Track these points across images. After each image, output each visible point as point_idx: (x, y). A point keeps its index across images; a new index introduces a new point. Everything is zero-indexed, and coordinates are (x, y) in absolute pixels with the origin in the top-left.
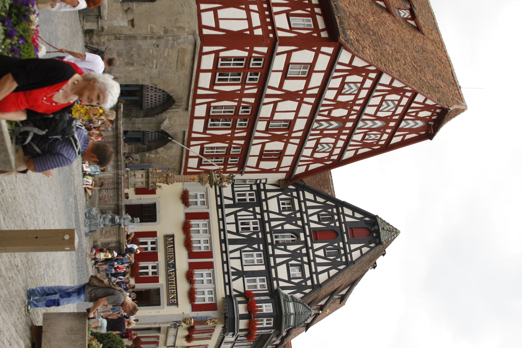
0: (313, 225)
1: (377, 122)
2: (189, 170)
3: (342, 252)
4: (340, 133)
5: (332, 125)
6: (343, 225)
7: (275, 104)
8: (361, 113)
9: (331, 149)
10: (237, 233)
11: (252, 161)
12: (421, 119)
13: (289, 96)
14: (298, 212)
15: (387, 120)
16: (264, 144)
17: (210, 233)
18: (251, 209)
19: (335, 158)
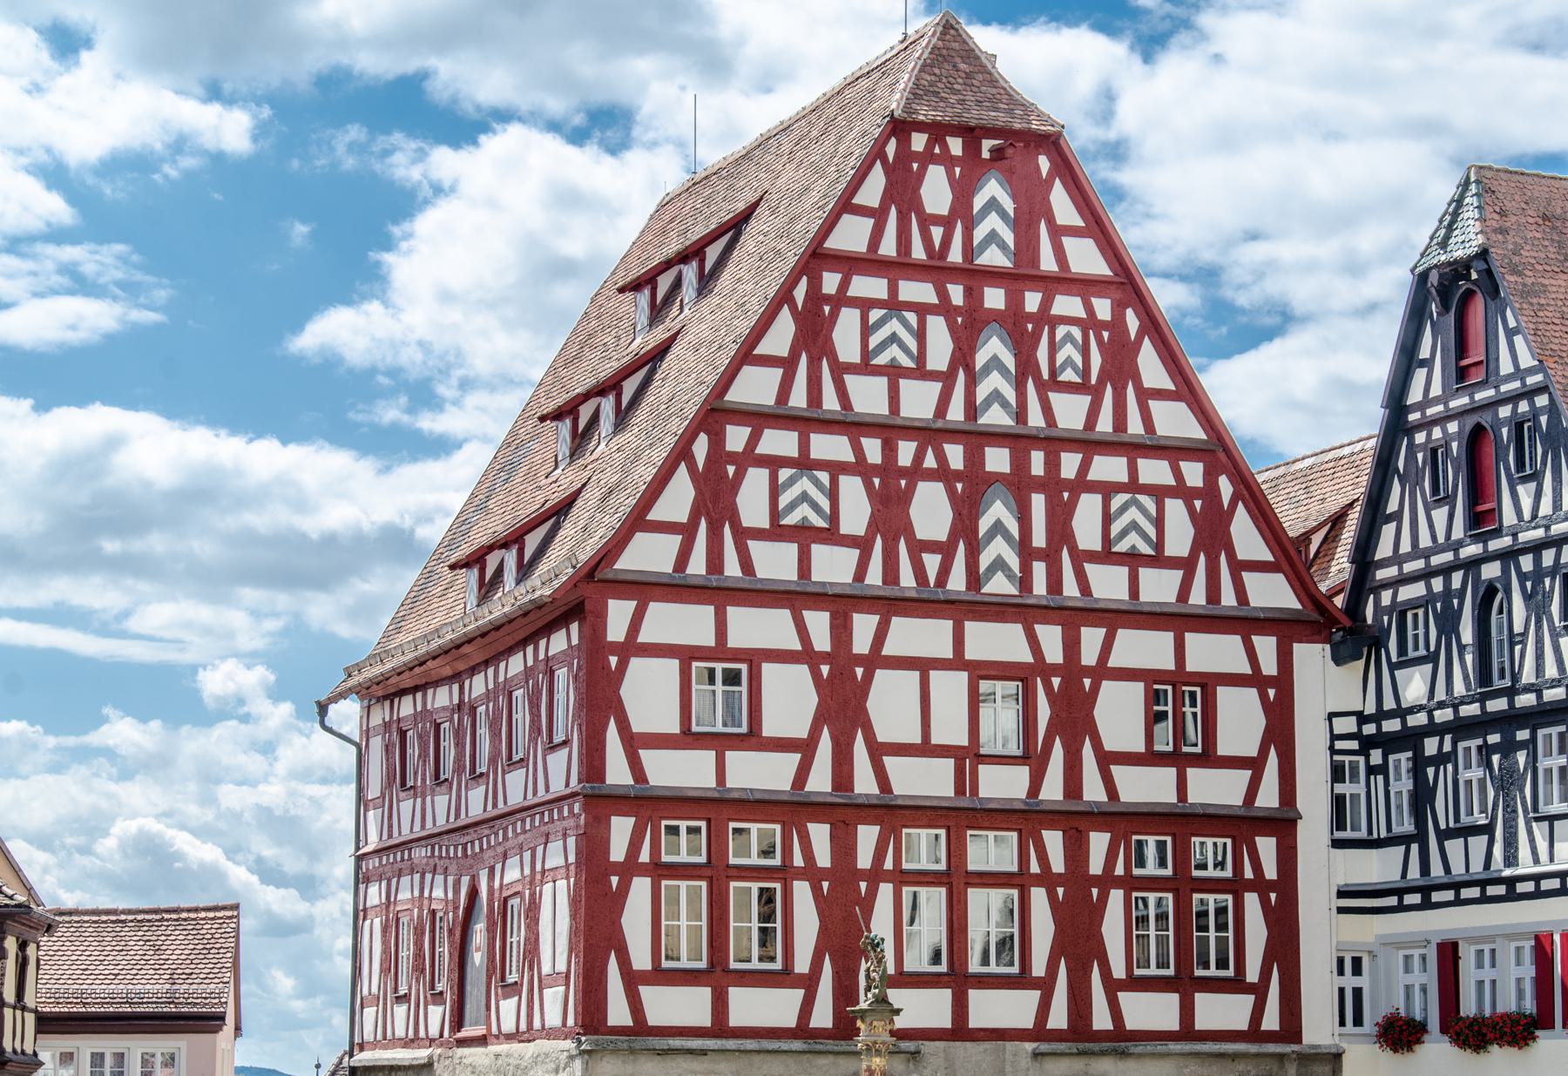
0: (1458, 532)
1: (981, 359)
2: (1271, 1021)
3: (1523, 406)
4: (1051, 483)
5: (998, 528)
6: (1452, 404)
7: (878, 751)
8: (930, 434)
9: (1145, 500)
10: (1488, 830)
11: (1216, 789)
12: (963, 192)
13: (843, 705)
14: (1429, 587)
15: (969, 328)
16: (1106, 760)
17: (1491, 939)
18: (1431, 771)
19: (1194, 473)
